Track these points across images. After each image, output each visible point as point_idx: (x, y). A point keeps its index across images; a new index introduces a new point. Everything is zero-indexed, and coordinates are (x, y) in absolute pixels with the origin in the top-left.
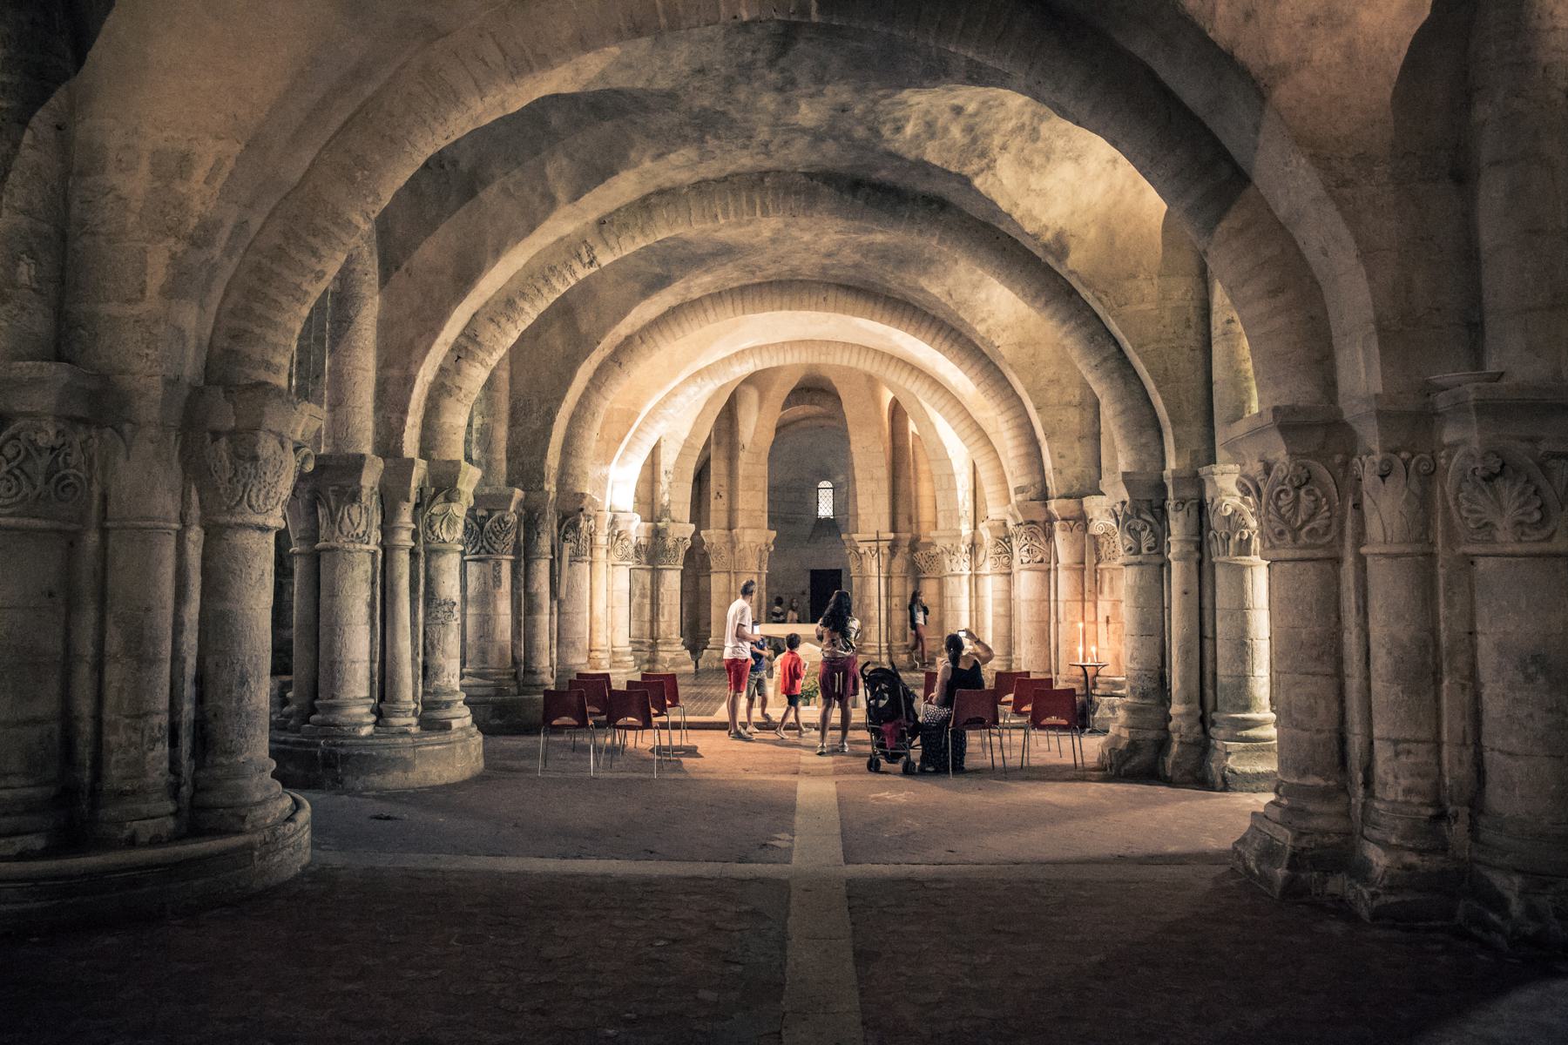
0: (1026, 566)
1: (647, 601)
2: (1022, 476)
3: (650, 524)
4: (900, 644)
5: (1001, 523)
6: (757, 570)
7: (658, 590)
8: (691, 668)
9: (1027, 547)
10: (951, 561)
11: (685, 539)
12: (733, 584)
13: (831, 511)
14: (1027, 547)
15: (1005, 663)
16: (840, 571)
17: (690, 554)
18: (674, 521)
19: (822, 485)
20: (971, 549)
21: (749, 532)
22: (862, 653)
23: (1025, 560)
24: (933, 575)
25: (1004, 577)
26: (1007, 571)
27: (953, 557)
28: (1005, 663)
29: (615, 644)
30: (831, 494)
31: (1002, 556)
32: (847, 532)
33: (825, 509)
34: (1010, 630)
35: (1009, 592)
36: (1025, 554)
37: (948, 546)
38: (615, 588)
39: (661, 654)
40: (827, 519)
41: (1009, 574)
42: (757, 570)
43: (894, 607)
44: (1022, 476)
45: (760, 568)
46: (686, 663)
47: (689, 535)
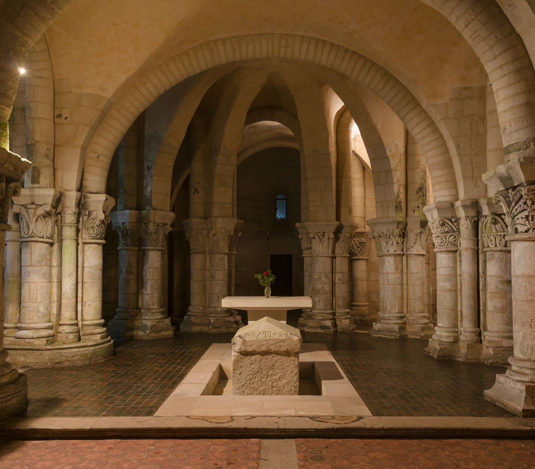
0: (525, 236)
1: (133, 277)
2: (517, 131)
3: (134, 212)
4: (343, 311)
5: (448, 205)
6: (227, 251)
7: (143, 268)
8: (170, 333)
9: (526, 213)
10: (387, 243)
11: (165, 224)
12: (208, 263)
13: (285, 215)
14: (526, 213)
15: (451, 334)
16: (291, 256)
17: (170, 237)
18: (155, 209)
19: (279, 196)
20: (404, 233)
21: (220, 220)
22: (312, 318)
23: (521, 228)
24: (363, 257)
25: (451, 254)
26: (454, 249)
27: (388, 240)
28: (451, 334)
29: (85, 317)
30: (285, 203)
31: (450, 234)
32: (299, 221)
33: (280, 215)
34: (456, 304)
35: (455, 268)
36: (521, 221)
37: (384, 232)
38: (86, 265)
39: (144, 322)
40: (282, 220)
41: (456, 251)
42: (227, 251)
43: (337, 281)
44: (517, 131)
45: (230, 250)
46: (168, 330)
47: (169, 222)
